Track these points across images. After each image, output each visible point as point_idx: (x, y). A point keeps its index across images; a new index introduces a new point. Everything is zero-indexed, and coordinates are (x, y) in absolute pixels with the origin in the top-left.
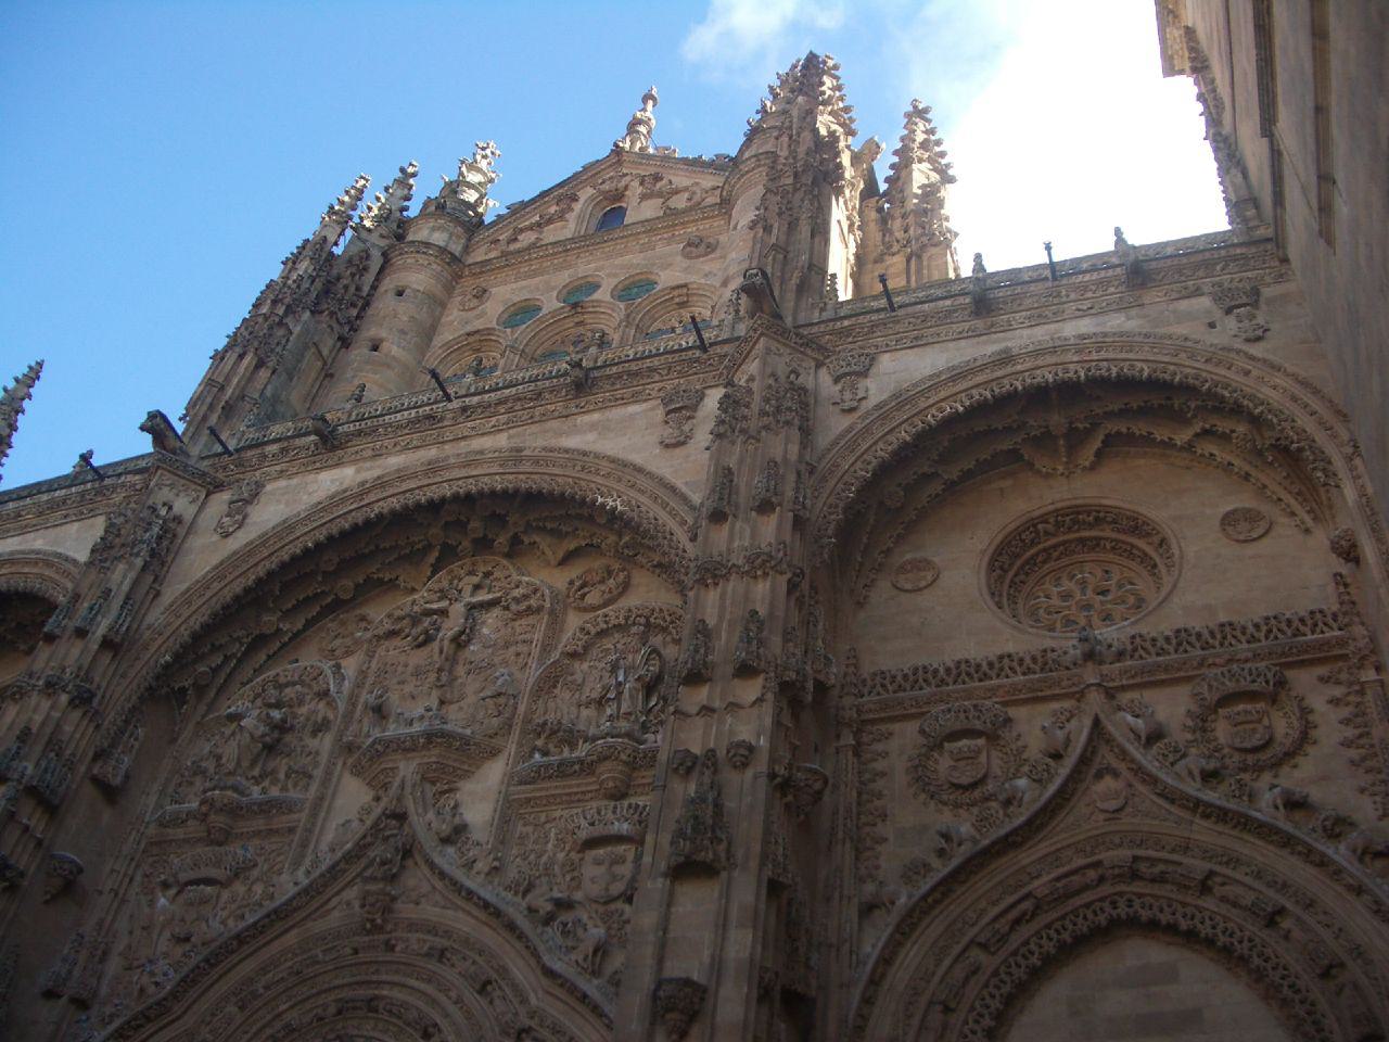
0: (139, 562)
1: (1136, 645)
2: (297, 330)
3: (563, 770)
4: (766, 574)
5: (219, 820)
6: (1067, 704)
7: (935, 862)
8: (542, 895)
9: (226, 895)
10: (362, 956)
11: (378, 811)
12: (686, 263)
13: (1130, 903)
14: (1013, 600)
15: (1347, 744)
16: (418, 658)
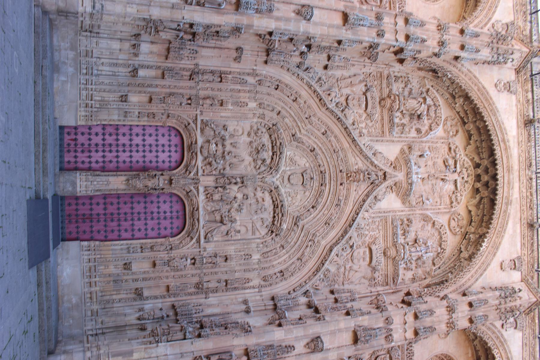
0: (490, 59)
3: (395, 234)
4: (448, 327)
8: (355, 241)
9: (361, 111)
11: (387, 170)
16: (440, 162)
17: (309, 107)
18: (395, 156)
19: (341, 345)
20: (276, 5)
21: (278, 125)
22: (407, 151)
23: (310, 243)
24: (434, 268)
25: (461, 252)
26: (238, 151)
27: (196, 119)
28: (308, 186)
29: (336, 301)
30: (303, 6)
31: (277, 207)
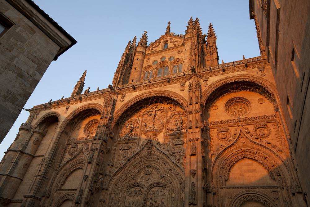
0: (111, 107)
1: (246, 119)
2: (125, 68)
6: (237, 127)
7: (221, 149)
9: (129, 151)
10: (148, 159)
13: (246, 155)
14: (228, 110)
15: (276, 135)
16: (149, 118)
17: (124, 172)
20: (81, 189)
26: (135, 201)
28: (150, 172)
30: (83, 178)
31: (156, 185)
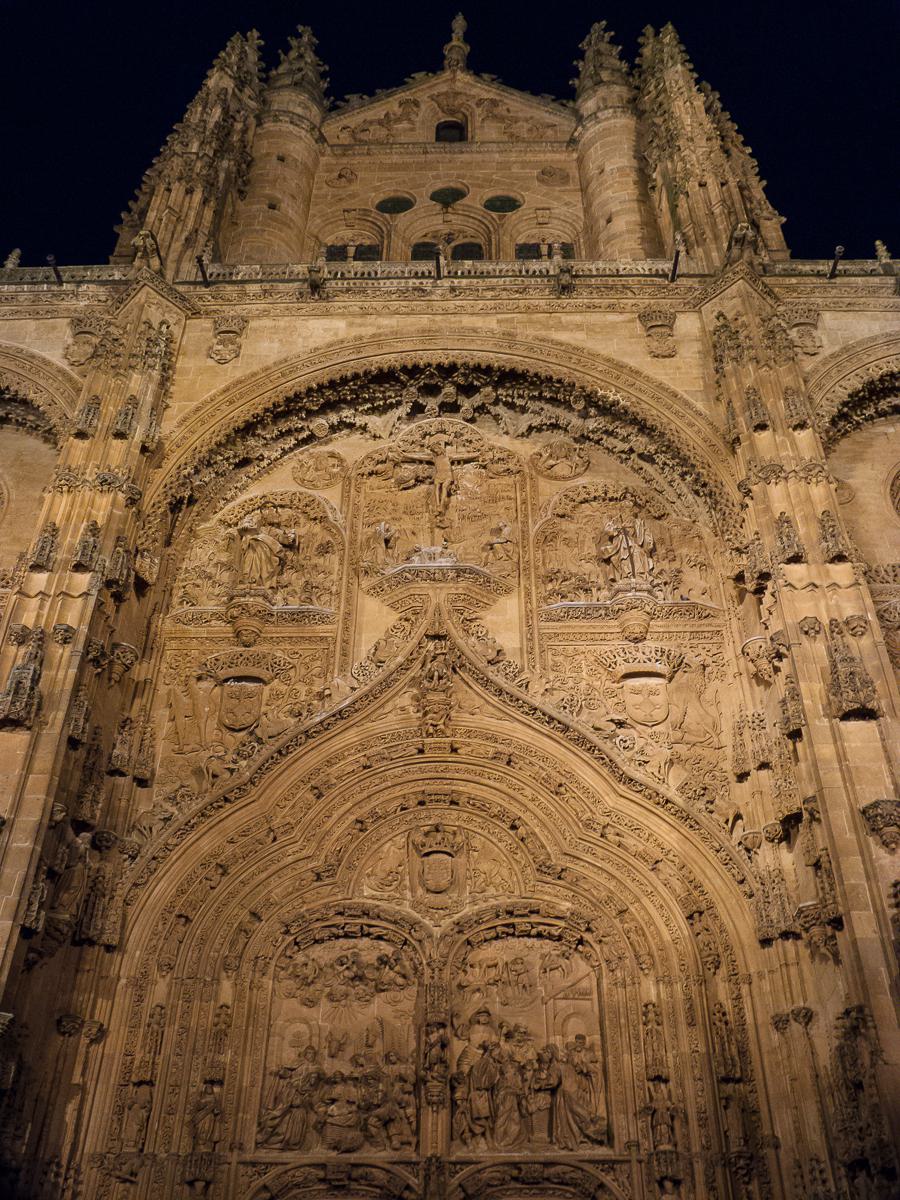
0: (156, 374)
5: (255, 623)
9: (267, 689)
11: (422, 630)
12: (545, 189)
18: (386, 609)
19: (882, 754)
21: (289, 918)
22: (374, 580)
23: (610, 837)
24: (674, 515)
25: (631, 450)
27: (254, 1164)
29: (764, 766)
31: (513, 926)
